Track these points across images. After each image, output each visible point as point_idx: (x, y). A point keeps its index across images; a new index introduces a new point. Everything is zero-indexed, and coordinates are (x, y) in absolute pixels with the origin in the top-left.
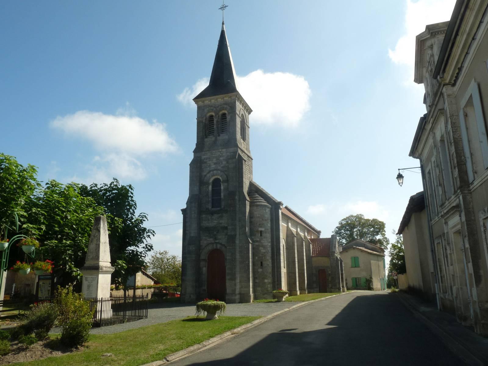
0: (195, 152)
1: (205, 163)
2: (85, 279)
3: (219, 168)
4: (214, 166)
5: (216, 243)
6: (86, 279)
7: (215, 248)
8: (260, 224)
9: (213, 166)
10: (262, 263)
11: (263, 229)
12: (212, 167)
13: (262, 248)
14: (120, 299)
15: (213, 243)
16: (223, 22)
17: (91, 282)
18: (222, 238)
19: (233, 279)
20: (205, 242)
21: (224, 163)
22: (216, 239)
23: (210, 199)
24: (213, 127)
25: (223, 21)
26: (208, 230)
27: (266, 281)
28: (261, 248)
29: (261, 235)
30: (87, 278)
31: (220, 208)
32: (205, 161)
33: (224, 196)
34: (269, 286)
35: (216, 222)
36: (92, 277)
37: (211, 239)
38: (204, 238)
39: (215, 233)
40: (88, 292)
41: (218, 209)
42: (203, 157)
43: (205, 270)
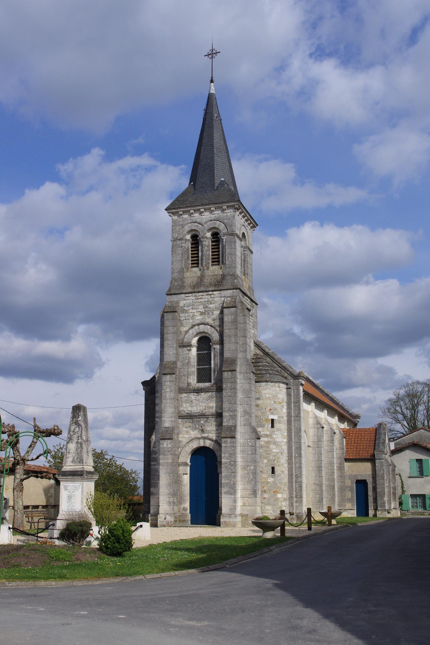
3: (209, 320)
5: (204, 438)
7: (202, 445)
8: (270, 410)
9: (199, 318)
10: (273, 468)
11: (275, 417)
12: (197, 318)
13: (274, 447)
15: (199, 438)
17: (73, 492)
19: (233, 491)
20: (186, 436)
25: (212, 77)
26: (190, 417)
27: (279, 496)
28: (272, 446)
29: (273, 426)
30: (67, 486)
32: (185, 308)
34: (284, 504)
36: (73, 486)
38: (184, 429)
40: (69, 504)
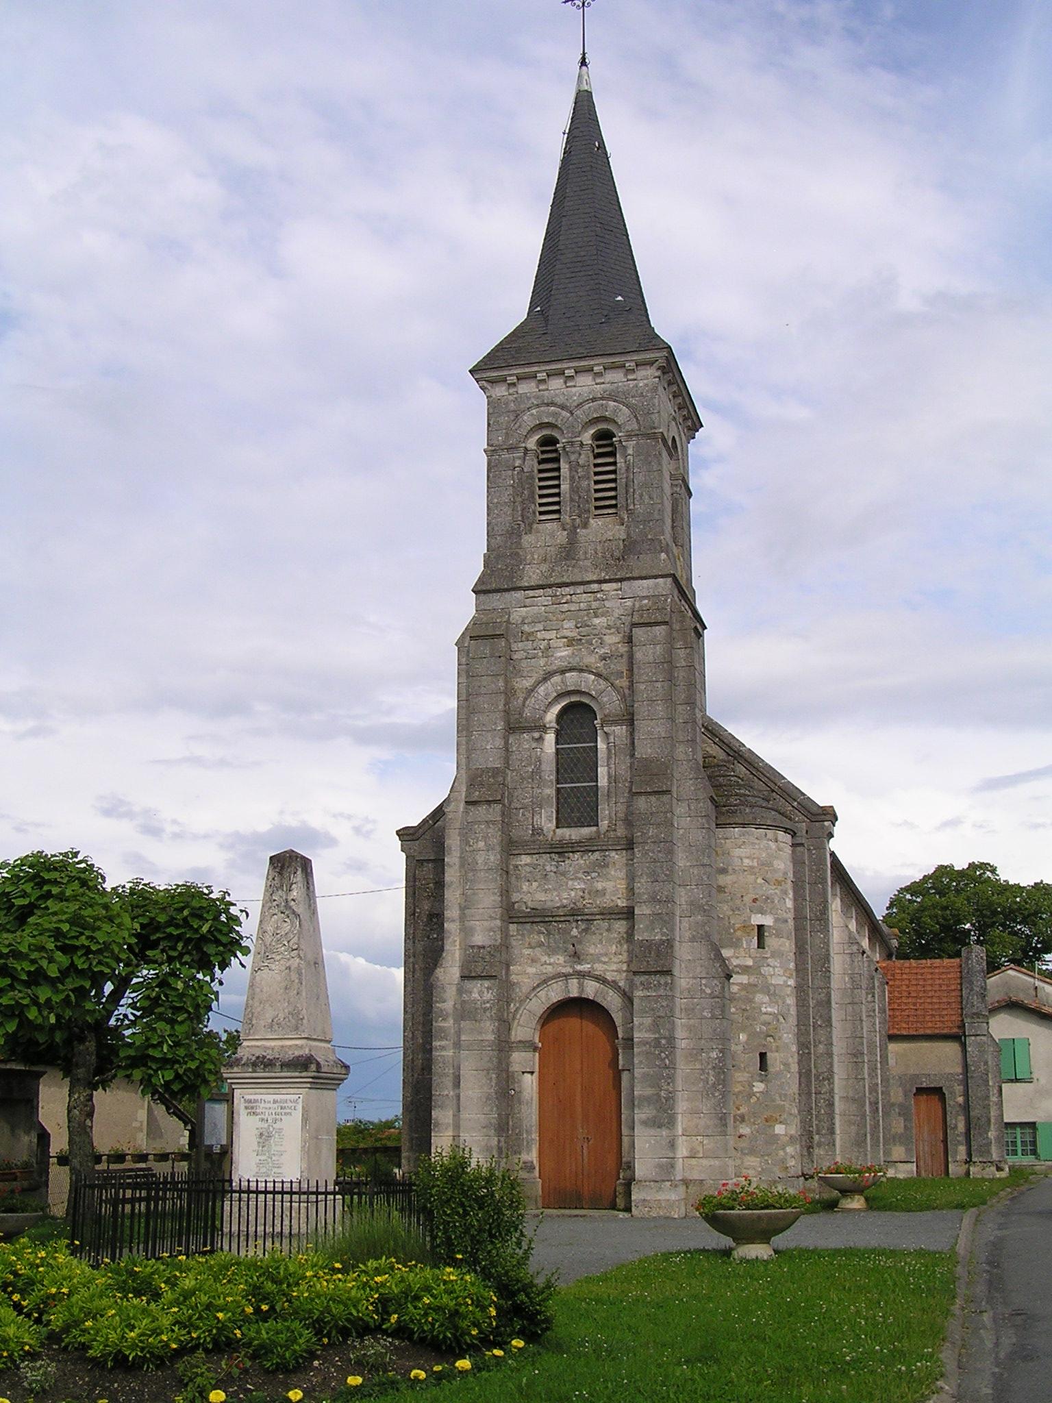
0: (480, 590)
1: (528, 637)
2: (246, 1108)
3: (591, 660)
4: (564, 653)
5: (581, 975)
6: (252, 1109)
7: (574, 993)
8: (755, 900)
9: (563, 654)
10: (763, 1056)
11: (767, 921)
12: (559, 654)
13: (766, 999)
14: (148, 1207)
15: (566, 976)
16: (584, 59)
17: (275, 1121)
18: (607, 957)
19: (664, 1118)
20: (531, 970)
21: (612, 639)
22: (576, 956)
23: (550, 791)
24: (558, 486)
25: (584, 54)
26: (540, 917)
27: (779, 1129)
28: (760, 998)
29: (761, 945)
30: (256, 1101)
31: (594, 829)
32: (526, 628)
33: (613, 779)
34: (789, 1150)
35: (579, 885)
36: (275, 1102)
37: (560, 959)
38: (526, 952)
39: (575, 932)
40: (264, 1158)
41: (586, 831)
42: (518, 614)
43: (529, 1085)
